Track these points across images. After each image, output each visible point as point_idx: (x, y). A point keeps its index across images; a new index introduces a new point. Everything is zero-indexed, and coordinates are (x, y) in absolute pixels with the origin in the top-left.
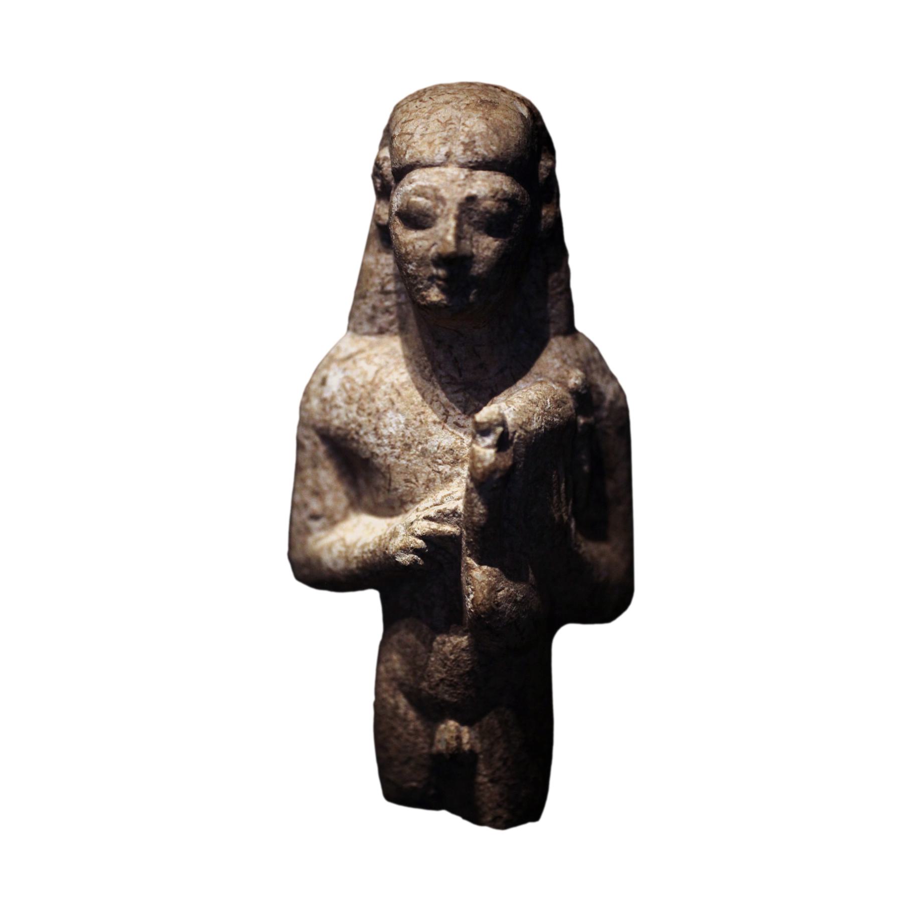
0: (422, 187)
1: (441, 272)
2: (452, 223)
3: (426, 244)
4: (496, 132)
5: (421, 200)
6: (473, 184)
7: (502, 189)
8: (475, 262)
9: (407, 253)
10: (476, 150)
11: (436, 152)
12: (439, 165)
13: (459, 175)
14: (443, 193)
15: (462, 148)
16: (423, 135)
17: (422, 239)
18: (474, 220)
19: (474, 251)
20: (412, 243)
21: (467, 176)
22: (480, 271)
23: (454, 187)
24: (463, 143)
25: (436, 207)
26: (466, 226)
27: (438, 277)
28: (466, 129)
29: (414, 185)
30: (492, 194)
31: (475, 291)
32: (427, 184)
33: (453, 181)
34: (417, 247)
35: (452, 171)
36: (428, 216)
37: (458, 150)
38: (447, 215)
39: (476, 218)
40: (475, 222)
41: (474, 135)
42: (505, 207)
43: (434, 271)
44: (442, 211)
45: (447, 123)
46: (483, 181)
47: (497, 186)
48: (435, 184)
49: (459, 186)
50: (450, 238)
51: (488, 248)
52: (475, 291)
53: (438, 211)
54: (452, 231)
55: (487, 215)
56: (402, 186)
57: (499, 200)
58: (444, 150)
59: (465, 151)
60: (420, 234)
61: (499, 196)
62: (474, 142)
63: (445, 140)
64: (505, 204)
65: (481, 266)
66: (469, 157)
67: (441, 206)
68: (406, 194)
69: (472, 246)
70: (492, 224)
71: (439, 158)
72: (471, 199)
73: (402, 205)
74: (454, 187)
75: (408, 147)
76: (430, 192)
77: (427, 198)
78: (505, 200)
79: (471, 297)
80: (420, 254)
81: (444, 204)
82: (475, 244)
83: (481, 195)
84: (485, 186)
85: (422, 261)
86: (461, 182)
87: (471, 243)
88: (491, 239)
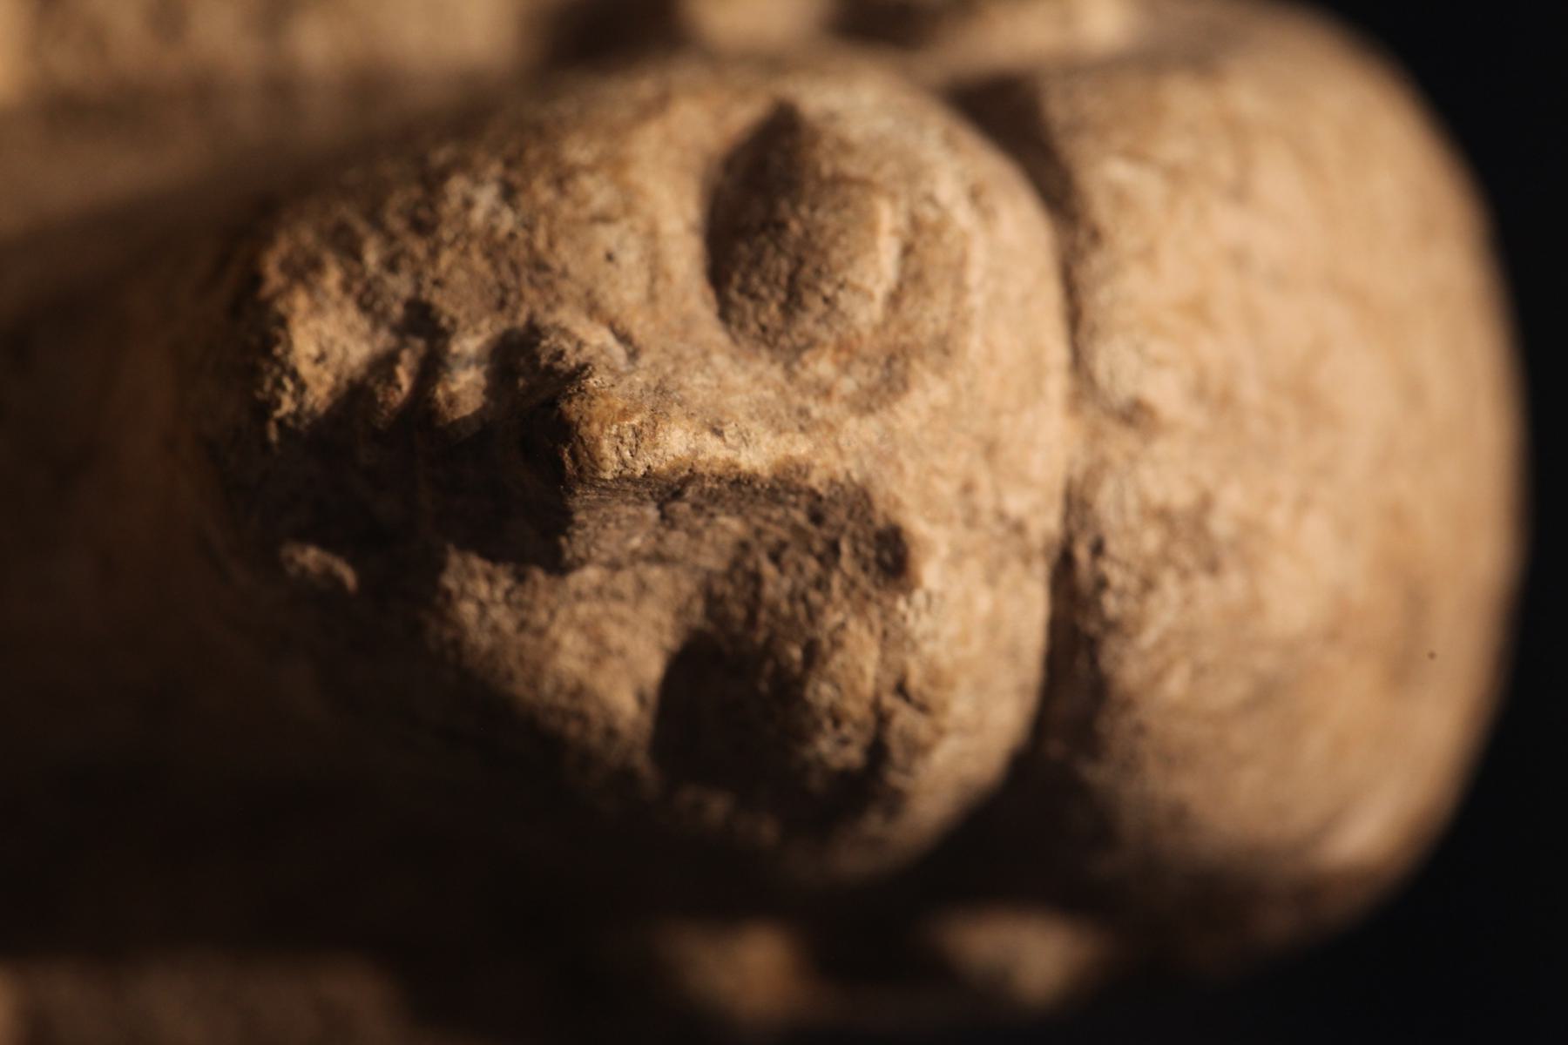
0: (959, 266)
1: (466, 386)
2: (758, 454)
3: (626, 291)
4: (1265, 694)
5: (879, 266)
6: (974, 567)
7: (940, 732)
8: (520, 578)
9: (562, 179)
10: (1169, 582)
11: (1156, 347)
12: (1079, 363)
13: (1024, 481)
14: (928, 393)
15: (1182, 498)
16: (1239, 259)
17: (656, 268)
18: (769, 570)
19: (591, 575)
20: (629, 209)
21: (1019, 528)
22: (468, 609)
23: (962, 460)
24: (1206, 503)
25: (847, 350)
26: (733, 525)
27: (432, 367)
28: (1278, 518)
29: (963, 216)
30: (915, 680)
31: (349, 576)
32: (976, 300)
33: (991, 449)
34: (607, 236)
35: (1048, 442)
36: (793, 304)
37: (1162, 475)
38: (804, 422)
39: (776, 584)
40: (756, 578)
41: (1251, 565)
42: (837, 750)
43: (469, 345)
44: (826, 392)
45: (1306, 397)
46: (993, 625)
47: (961, 706)
48: (974, 343)
49: (968, 488)
50: (677, 443)
51: (601, 652)
52: (349, 576)
53: (822, 367)
54: (715, 451)
55: (796, 653)
56: (949, 141)
57: (882, 718)
58: (1165, 392)
59: (1163, 516)
60: (684, 255)
61: (904, 717)
62: (1213, 567)
63: (1217, 398)
64: (853, 755)
65: (498, 613)
66: (1131, 541)
67: (847, 385)
68: (914, 173)
69: (614, 566)
70: (736, 679)
71: (1122, 365)
72: (892, 559)
73: (845, 147)
74: (962, 460)
75: (1175, 175)
76: (932, 315)
77: (895, 299)
78: (878, 751)
79: (311, 557)
80: (565, 254)
81: (865, 404)
82: (625, 581)
83: (915, 616)
84: (965, 639)
85: (523, 266)
86: (984, 500)
87: (635, 555)
88: (653, 668)
